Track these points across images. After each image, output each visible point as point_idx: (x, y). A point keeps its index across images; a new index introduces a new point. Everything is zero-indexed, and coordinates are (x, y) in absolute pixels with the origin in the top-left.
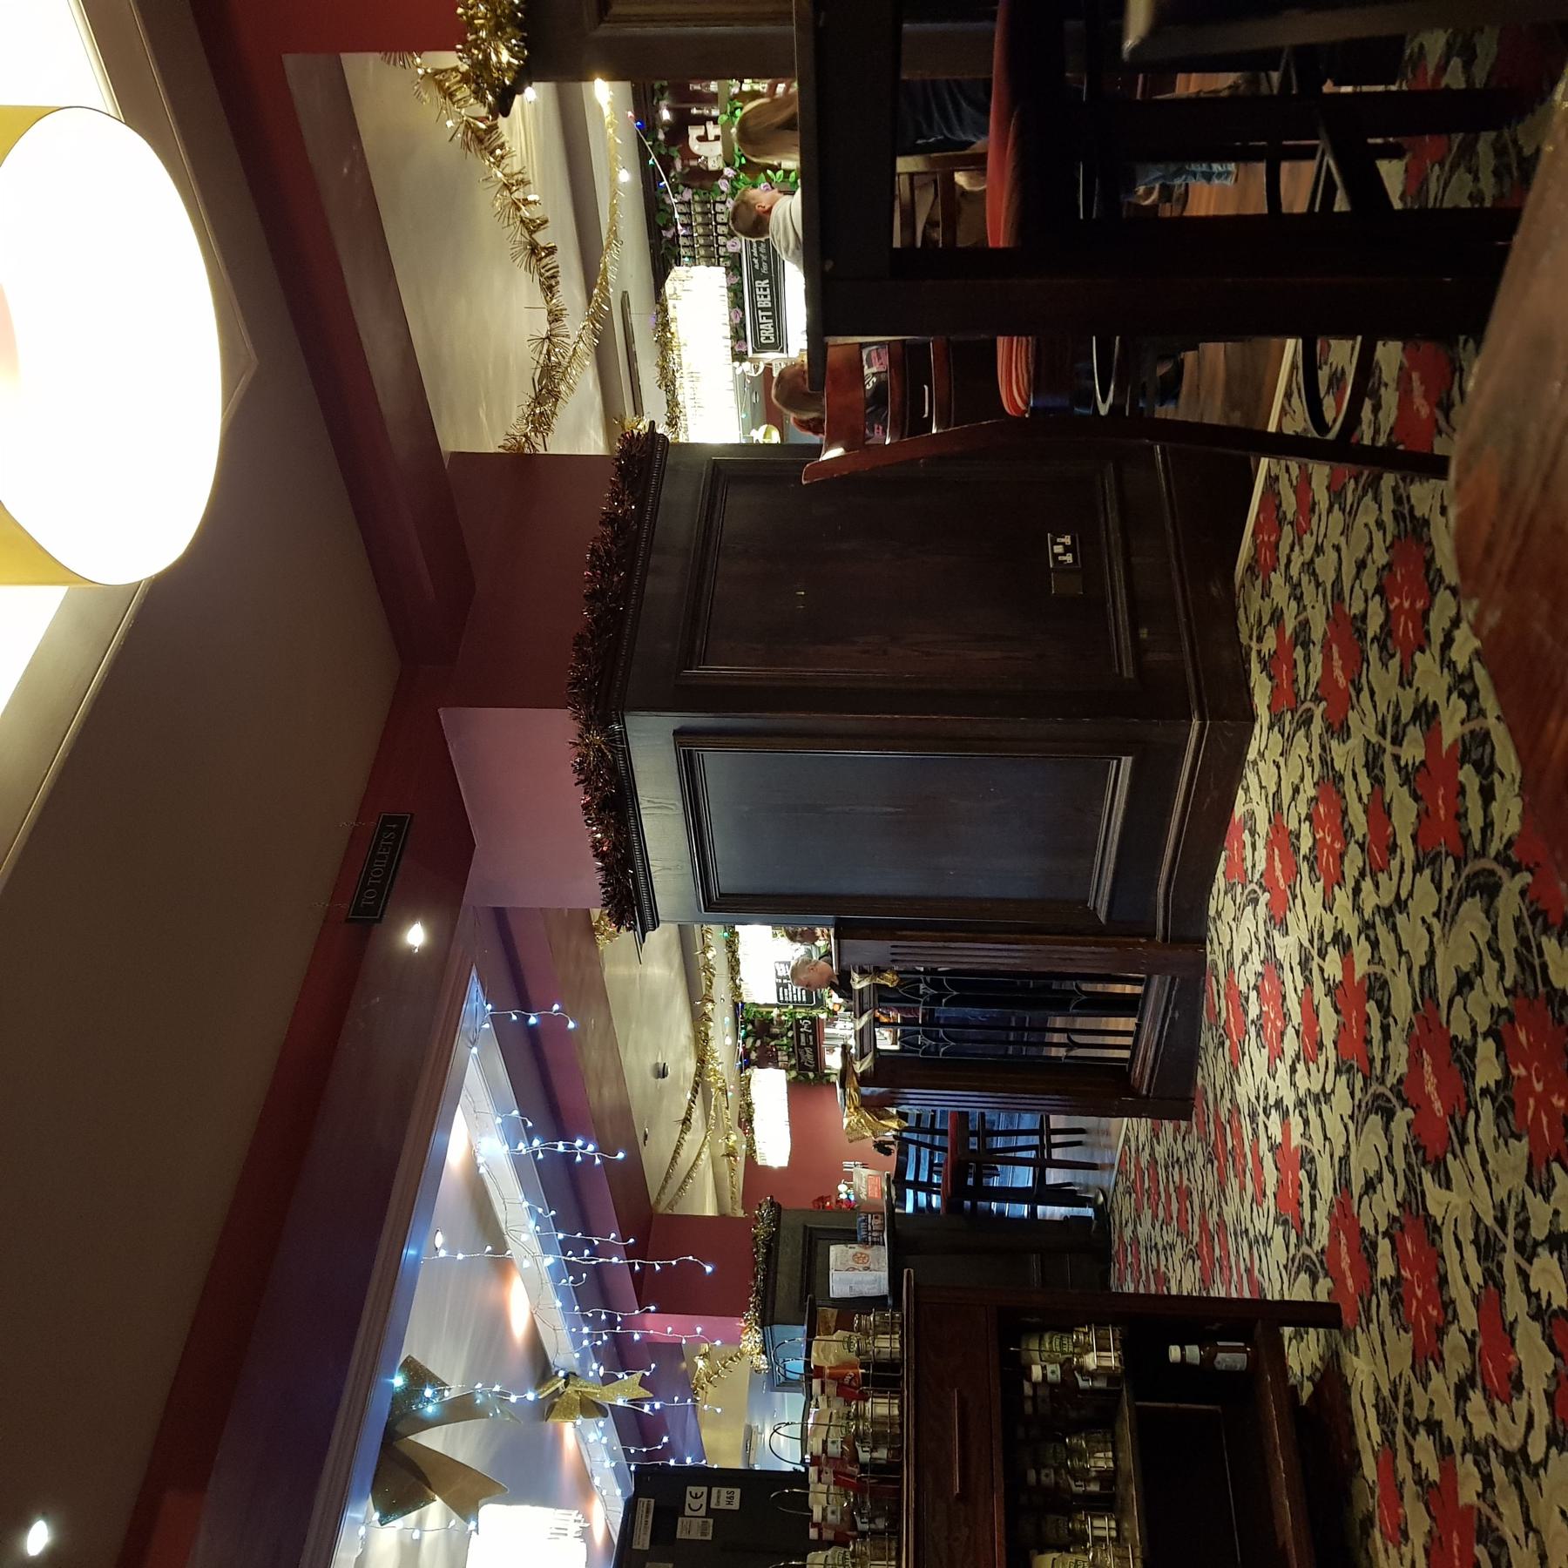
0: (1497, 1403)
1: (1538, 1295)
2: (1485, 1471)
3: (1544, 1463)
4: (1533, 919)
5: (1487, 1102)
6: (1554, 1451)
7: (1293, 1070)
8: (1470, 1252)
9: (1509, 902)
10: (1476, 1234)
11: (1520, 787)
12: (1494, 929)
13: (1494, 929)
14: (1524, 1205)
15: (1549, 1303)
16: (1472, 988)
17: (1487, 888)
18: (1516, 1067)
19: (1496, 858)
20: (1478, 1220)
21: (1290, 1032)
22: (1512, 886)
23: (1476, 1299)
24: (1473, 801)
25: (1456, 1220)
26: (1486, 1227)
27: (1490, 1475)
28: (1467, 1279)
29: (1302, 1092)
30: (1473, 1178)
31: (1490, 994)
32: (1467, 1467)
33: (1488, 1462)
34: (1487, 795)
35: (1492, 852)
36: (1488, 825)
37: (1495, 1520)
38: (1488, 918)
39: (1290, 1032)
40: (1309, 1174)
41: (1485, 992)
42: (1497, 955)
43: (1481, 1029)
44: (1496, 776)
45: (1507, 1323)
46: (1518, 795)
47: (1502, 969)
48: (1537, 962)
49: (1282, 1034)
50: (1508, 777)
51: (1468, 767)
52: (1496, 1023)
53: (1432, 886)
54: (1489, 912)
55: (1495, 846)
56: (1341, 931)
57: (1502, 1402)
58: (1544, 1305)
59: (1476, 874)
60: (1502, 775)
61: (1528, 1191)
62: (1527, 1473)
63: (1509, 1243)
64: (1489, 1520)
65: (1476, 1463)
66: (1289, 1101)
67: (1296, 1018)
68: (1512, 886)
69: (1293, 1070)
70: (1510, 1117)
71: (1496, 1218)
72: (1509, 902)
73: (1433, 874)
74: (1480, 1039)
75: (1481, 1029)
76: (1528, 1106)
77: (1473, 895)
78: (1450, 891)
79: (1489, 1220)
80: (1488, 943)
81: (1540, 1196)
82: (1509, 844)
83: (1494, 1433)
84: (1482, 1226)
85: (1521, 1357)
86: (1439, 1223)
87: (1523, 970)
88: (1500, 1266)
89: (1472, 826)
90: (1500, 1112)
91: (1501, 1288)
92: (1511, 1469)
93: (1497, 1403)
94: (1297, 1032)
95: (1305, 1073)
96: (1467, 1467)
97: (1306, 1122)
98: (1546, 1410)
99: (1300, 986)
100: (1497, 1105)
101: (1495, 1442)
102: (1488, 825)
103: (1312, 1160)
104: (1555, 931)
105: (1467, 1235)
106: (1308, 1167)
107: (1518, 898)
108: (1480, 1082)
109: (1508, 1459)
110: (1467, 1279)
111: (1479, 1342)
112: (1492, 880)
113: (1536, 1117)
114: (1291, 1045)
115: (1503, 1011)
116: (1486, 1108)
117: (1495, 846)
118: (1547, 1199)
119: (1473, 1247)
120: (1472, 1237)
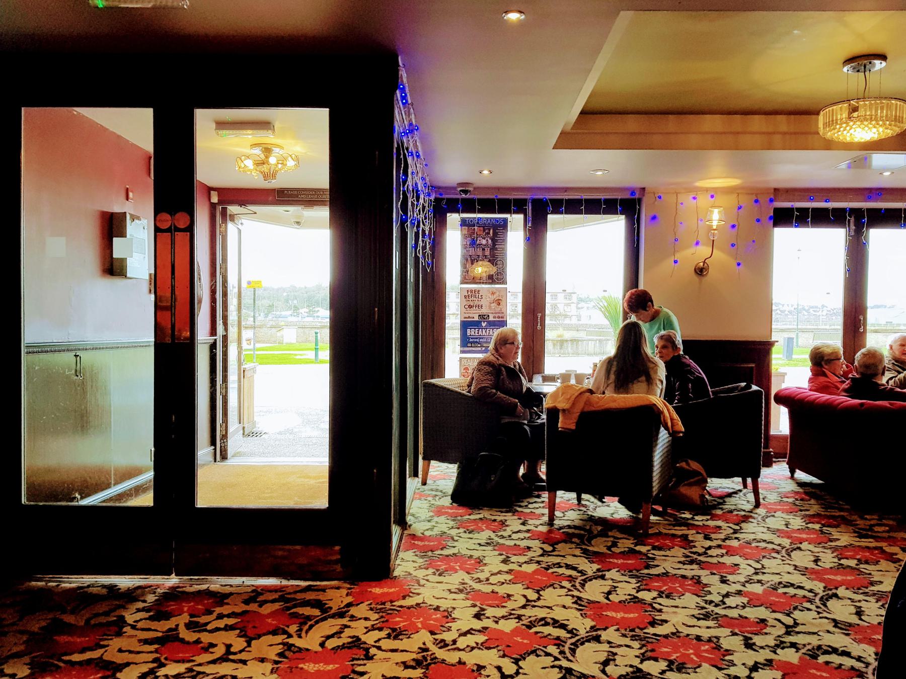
0: (765, 631)
2: (788, 645)
3: (795, 620)
6: (792, 615)
27: (791, 643)
32: (750, 588)
33: (785, 642)
37: (809, 647)
57: (765, 628)
61: (725, 672)
62: (796, 627)
64: (809, 650)
65: (783, 648)
83: (774, 636)
92: (792, 633)
93: (765, 631)
96: (750, 588)
98: (777, 614)
100: (675, 670)
101: (779, 636)
109: (788, 633)
111: (737, 631)
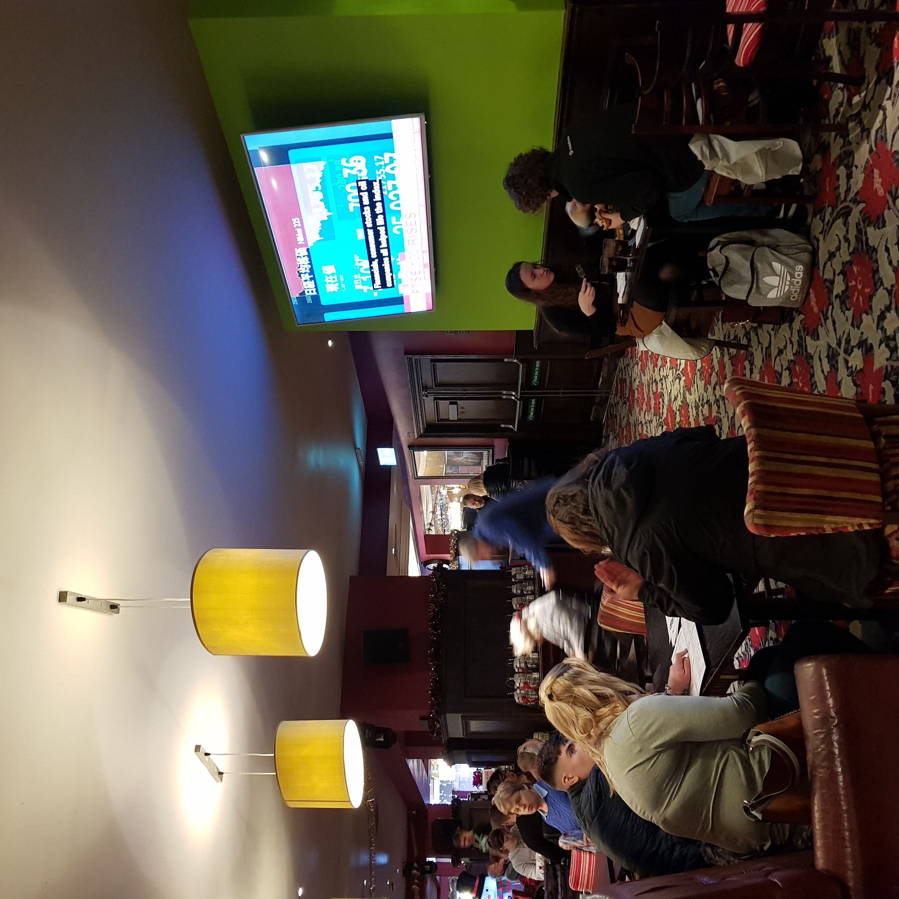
1: (852, 367)
4: (864, 222)
5: (838, 300)
7: (714, 389)
8: (825, 361)
9: (855, 216)
10: (828, 354)
11: (864, 169)
12: (847, 230)
13: (847, 230)
14: (849, 334)
15: (856, 368)
16: (835, 257)
17: (847, 213)
18: (851, 282)
19: (850, 201)
20: (829, 346)
21: (714, 374)
22: (856, 210)
23: (826, 378)
24: (843, 181)
25: (820, 351)
26: (833, 348)
28: (823, 371)
29: (717, 397)
30: (829, 332)
31: (844, 255)
34: (849, 176)
35: (849, 199)
36: (848, 190)
38: (845, 226)
39: (714, 374)
40: (719, 426)
41: (841, 257)
42: (847, 239)
43: (837, 272)
44: (854, 168)
45: (838, 382)
46: (863, 172)
47: (849, 245)
48: (864, 239)
49: (711, 375)
50: (859, 166)
51: (842, 168)
52: (844, 268)
53: (820, 221)
54: (845, 223)
55: (852, 195)
56: (737, 336)
58: (854, 370)
59: (841, 209)
60: (857, 167)
61: (852, 328)
63: (841, 351)
66: (712, 400)
67: (717, 368)
68: (856, 210)
69: (714, 389)
70: (847, 302)
71: (837, 344)
72: (855, 216)
73: (821, 217)
74: (836, 276)
75: (837, 272)
76: (854, 295)
77: (839, 218)
78: (829, 221)
79: (834, 345)
80: (844, 237)
81: (856, 329)
82: (857, 194)
84: (831, 349)
85: (843, 393)
86: (812, 355)
87: (858, 243)
88: (837, 362)
89: (841, 191)
90: (843, 303)
91: (837, 369)
94: (717, 374)
95: (719, 389)
97: (719, 407)
99: (719, 356)
102: (848, 190)
103: (721, 420)
104: (873, 224)
105: (824, 354)
106: (719, 423)
107: (859, 214)
108: (835, 293)
110: (823, 371)
112: (848, 210)
113: (858, 299)
114: (714, 379)
115: (847, 262)
116: (837, 303)
117: (852, 195)
118: (858, 328)
119: (826, 359)
120: (826, 354)
